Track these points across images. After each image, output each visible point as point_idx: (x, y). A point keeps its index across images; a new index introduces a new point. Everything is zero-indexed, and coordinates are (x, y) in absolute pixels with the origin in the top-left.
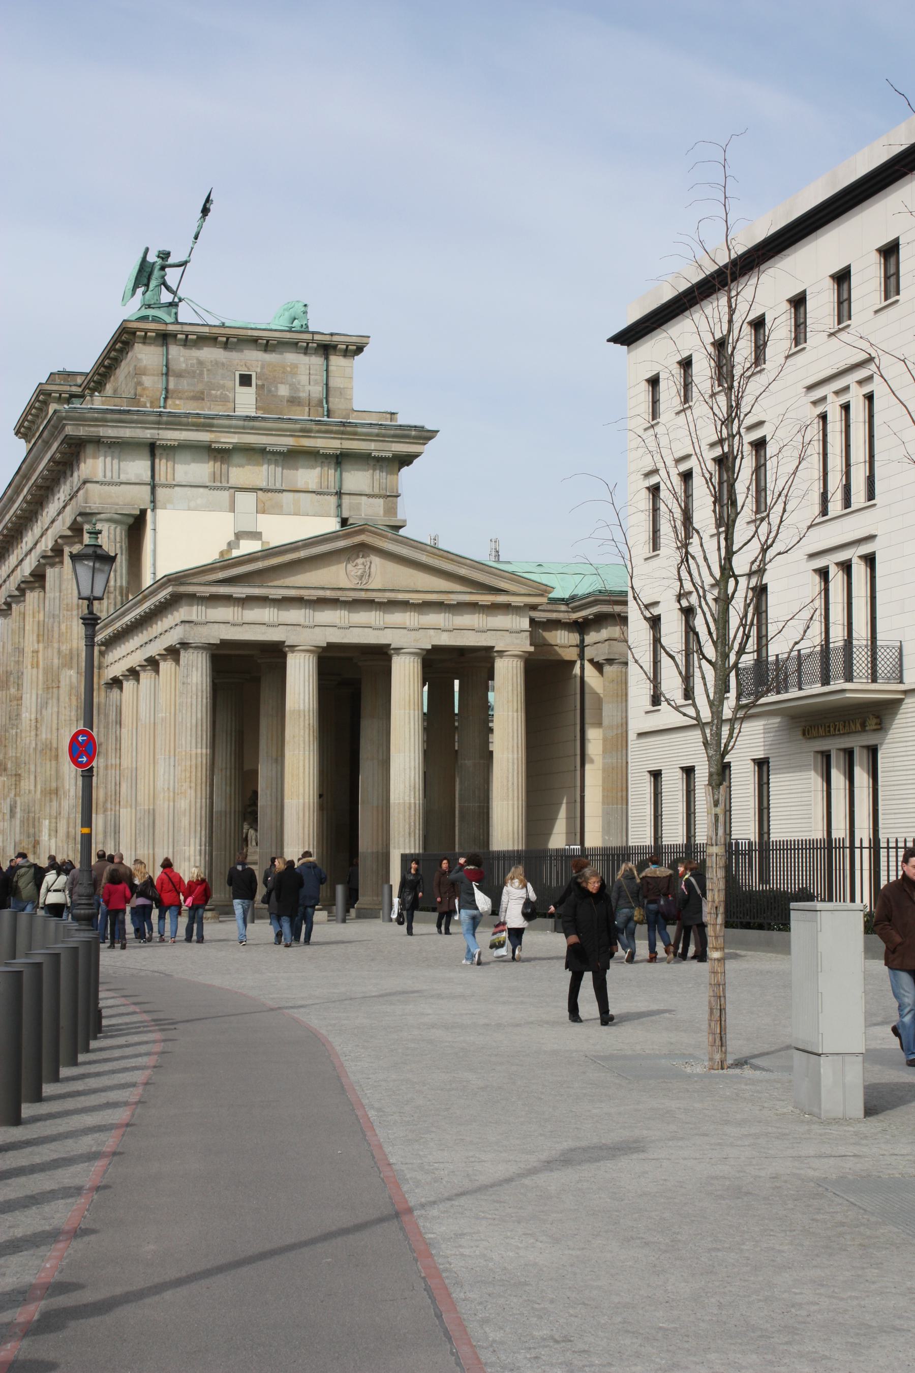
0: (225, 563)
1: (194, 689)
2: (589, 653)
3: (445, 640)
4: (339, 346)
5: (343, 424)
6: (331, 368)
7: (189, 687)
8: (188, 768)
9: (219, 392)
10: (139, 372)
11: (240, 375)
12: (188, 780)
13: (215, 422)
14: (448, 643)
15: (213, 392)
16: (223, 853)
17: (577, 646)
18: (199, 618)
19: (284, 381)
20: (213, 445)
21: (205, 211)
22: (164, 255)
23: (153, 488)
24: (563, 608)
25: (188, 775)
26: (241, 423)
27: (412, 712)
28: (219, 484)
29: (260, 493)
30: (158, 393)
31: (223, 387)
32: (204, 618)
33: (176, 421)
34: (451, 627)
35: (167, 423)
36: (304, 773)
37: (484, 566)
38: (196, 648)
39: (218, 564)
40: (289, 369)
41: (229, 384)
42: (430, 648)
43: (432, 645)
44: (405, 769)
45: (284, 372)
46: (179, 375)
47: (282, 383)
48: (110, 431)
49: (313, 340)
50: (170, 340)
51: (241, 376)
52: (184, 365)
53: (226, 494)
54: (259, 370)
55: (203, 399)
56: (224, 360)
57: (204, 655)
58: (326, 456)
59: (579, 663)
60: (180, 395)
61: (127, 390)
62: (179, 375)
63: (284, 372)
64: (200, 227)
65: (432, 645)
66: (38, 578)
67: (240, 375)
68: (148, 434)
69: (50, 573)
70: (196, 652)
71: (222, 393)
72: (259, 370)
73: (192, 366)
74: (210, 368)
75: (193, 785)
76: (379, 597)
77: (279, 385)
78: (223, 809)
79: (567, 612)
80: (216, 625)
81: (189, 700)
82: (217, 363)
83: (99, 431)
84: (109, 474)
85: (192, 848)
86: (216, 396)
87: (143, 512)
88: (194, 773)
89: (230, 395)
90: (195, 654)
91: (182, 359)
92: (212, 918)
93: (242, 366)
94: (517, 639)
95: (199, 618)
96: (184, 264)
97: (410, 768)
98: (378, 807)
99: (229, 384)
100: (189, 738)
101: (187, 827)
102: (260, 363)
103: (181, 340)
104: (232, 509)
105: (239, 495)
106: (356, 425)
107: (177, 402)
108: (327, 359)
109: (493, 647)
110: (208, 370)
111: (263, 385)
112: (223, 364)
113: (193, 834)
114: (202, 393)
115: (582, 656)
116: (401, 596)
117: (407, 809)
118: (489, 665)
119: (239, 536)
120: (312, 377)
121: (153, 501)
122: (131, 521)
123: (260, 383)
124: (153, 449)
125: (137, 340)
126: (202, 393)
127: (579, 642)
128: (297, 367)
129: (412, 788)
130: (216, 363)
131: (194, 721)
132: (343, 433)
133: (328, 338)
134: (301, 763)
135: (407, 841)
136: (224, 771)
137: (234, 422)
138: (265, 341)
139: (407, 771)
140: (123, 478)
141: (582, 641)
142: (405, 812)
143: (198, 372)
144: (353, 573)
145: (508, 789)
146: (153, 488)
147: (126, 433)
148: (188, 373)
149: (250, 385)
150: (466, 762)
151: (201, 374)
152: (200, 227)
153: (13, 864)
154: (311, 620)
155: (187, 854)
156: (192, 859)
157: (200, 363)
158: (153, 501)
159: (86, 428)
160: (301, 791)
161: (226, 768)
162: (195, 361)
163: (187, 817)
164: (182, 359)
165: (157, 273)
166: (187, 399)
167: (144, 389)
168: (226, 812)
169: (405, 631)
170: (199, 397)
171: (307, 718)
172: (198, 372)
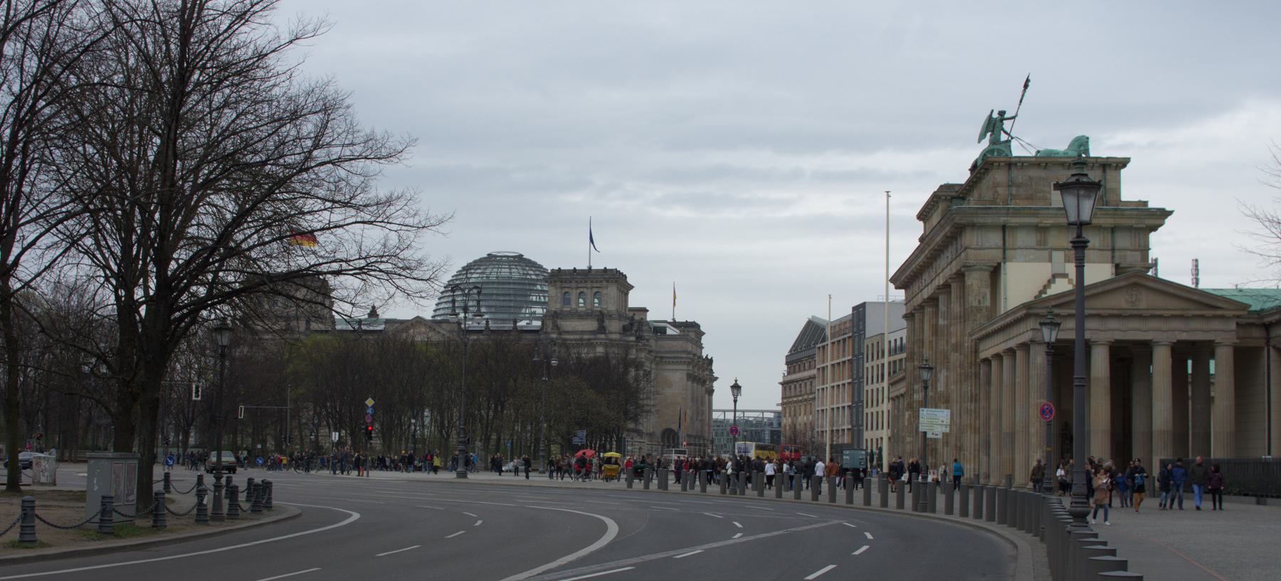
2: (1272, 342)
3: (1184, 336)
5: (1116, 210)
10: (996, 185)
13: (1040, 212)
15: (1038, 195)
20: (1039, 225)
21: (1026, 86)
22: (1002, 113)
23: (1004, 250)
26: (1055, 212)
28: (1042, 247)
29: (1066, 251)
33: (1017, 212)
35: (1013, 213)
50: (1013, 167)
53: (1046, 253)
58: (1106, 229)
61: (988, 195)
62: (1018, 186)
64: (1023, 95)
66: (933, 300)
68: (1002, 220)
69: (942, 298)
84: (980, 244)
87: (999, 264)
96: (1013, 118)
104: (1050, 260)
105: (1054, 253)
106: (1123, 210)
107: (1018, 201)
108: (1104, 171)
112: (1043, 178)
116: (1158, 313)
119: (1054, 276)
121: (1004, 258)
122: (992, 269)
124: (1004, 228)
132: (1115, 215)
133: (1106, 160)
137: (1051, 211)
140: (987, 245)
146: (1004, 250)
147: (989, 220)
152: (1023, 95)
157: (1031, 178)
158: (1004, 258)
162: (1027, 178)
165: (998, 124)
170: (1030, 198)
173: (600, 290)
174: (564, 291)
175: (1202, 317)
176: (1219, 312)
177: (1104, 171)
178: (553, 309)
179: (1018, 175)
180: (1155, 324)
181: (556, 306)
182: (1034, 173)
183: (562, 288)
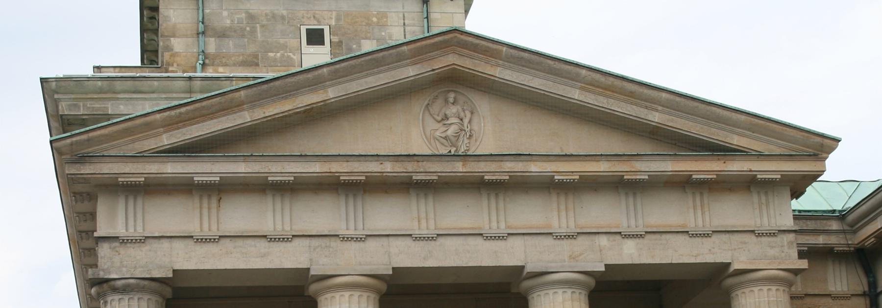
0: (173, 113)
6: (433, 16)
9: (279, 55)
11: (307, 30)
14: (637, 261)
15: (271, 55)
17: (864, 295)
18: (131, 230)
19: (369, 35)
24: (835, 226)
30: (194, 60)
31: (284, 47)
32: (140, 229)
34: (641, 229)
37: (696, 104)
38: (126, 290)
39: (158, 116)
40: (375, 20)
41: (294, 43)
42: (603, 269)
45: (368, 24)
46: (222, 35)
47: (366, 38)
48: (122, 107)
51: (309, 32)
52: (228, 22)
54: (333, 23)
55: (257, 65)
56: (285, 13)
60: (224, 60)
62: (222, 35)
63: (368, 24)
65: (606, 265)
67: (307, 30)
70: (126, 298)
71: (283, 55)
72: (333, 23)
73: (240, 21)
74: (265, 22)
76: (490, 170)
77: (362, 41)
79: (843, 232)
80: (165, 244)
82: (274, 16)
83: (107, 108)
86: (275, 60)
89: (295, 57)
93: (309, 18)
94: (773, 247)
95: (131, 230)
99: (294, 43)
102: (334, 14)
109: (728, 265)
110: (262, 26)
111: (341, 42)
112: (283, 18)
114: (256, 56)
116: (535, 168)
120: (407, 28)
123: (335, 39)
126: (256, 56)
127: (866, 289)
141: (873, 285)
143: (248, 29)
144: (438, 134)
148: (235, 31)
149: (321, 42)
151: (253, 31)
154: (360, 226)
157: (251, 17)
159: (89, 103)
162: (243, 15)
164: (225, 13)
166: (234, 65)
167: (174, 55)
169: (548, 241)
170: (252, 62)
176: (736, 166)
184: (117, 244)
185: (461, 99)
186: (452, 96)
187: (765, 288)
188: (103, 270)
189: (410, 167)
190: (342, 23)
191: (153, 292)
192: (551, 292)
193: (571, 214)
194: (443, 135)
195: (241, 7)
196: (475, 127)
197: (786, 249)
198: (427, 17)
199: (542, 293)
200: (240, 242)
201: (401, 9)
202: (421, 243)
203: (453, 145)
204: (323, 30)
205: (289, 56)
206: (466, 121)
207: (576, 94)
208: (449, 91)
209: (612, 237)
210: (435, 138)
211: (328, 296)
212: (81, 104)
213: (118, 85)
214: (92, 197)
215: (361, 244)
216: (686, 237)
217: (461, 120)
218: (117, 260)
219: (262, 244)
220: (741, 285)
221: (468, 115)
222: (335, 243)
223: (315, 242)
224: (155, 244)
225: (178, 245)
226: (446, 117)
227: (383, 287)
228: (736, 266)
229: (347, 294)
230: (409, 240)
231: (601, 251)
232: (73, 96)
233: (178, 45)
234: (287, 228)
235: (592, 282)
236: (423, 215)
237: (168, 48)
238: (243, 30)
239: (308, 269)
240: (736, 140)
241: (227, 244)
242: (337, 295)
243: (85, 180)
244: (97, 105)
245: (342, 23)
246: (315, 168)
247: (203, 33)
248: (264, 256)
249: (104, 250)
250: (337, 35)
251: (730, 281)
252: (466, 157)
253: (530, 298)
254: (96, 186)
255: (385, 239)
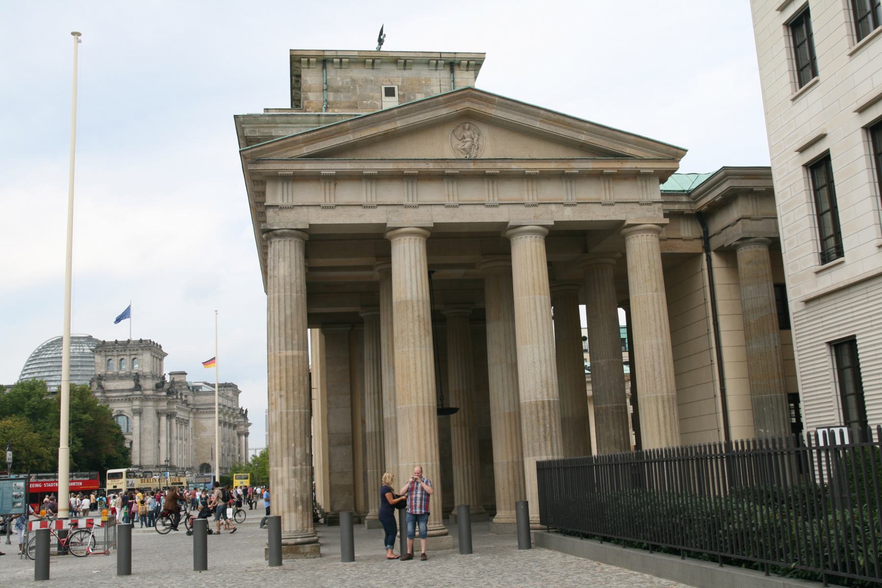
0: (309, 135)
1: (282, 282)
2: (715, 243)
3: (568, 215)
4: (462, 61)
6: (457, 80)
7: (276, 280)
8: (278, 374)
9: (369, 102)
11: (385, 88)
12: (278, 387)
14: (572, 219)
15: (365, 102)
16: (375, 470)
17: (701, 238)
18: (286, 202)
24: (684, 199)
25: (278, 381)
27: (538, 296)
30: (321, 105)
31: (372, 98)
32: (290, 201)
34: (574, 201)
36: (416, 372)
37: (605, 130)
38: (282, 235)
39: (300, 137)
40: (423, 82)
41: (377, 95)
42: (553, 224)
43: (555, 222)
44: (534, 362)
46: (337, 91)
47: (418, 93)
48: (280, 132)
49: (441, 57)
50: (329, 66)
52: (340, 83)
55: (357, 108)
56: (372, 78)
57: (293, 244)
59: (704, 255)
60: (338, 105)
62: (337, 91)
65: (555, 222)
67: (385, 88)
70: (283, 240)
71: (371, 102)
73: (347, 83)
74: (361, 84)
75: (283, 393)
76: (488, 167)
78: (374, 430)
79: (689, 202)
80: (305, 209)
81: (276, 294)
82: (366, 80)
83: (272, 132)
85: (285, 468)
86: (367, 105)
88: (284, 380)
90: (282, 243)
91: (339, 79)
92: (311, 553)
93: (386, 81)
94: (649, 211)
95: (286, 202)
97: (540, 361)
98: (510, 413)
99: (377, 95)
100: (277, 339)
101: (279, 443)
102: (401, 78)
103: (337, 63)
108: (452, 71)
110: (360, 86)
111: (404, 95)
112: (371, 81)
113: (285, 452)
114: (356, 103)
115: (707, 249)
116: (514, 166)
117: (540, 408)
118: (619, 255)
120: (442, 87)
123: (401, 93)
125: (303, 66)
127: (702, 235)
128: (430, 81)
129: (544, 384)
130: (366, 81)
131: (282, 319)
133: (452, 55)
134: (412, 362)
135: (543, 445)
136: (372, 395)
138: (403, 61)
139: (537, 365)
141: (706, 232)
142: (538, 413)
143: (352, 87)
144: (459, 147)
145: (655, 379)
148: (344, 89)
149: (394, 95)
150: (599, 361)
151: (355, 89)
153: (243, 488)
154: (415, 199)
155: (280, 476)
156: (286, 481)
157: (354, 81)
159: (261, 130)
160: (414, 394)
161: (374, 393)
162: (349, 80)
163: (278, 433)
164: (339, 79)
166: (344, 108)
167: (310, 102)
168: (376, 432)
169: (522, 208)
170: (354, 106)
171: (416, 308)
172: (352, 87)
173: (137, 357)
174: (108, 359)
175: (599, 176)
176: (629, 165)
177: (452, 71)
178: (99, 373)
179: (336, 76)
180: (510, 191)
181: (101, 371)
182: (358, 73)
183: (106, 356)
184: (277, 210)
185: (473, 127)
186: (467, 126)
187: (645, 235)
188: (270, 224)
189: (444, 165)
190: (405, 84)
191: (298, 237)
192: (523, 237)
193: (535, 193)
194: (462, 148)
195: (347, 75)
196: (481, 143)
197: (657, 213)
198: (453, 81)
199: (519, 237)
200: (347, 208)
201: (438, 76)
202: (450, 209)
203: (468, 153)
204: (394, 88)
205: (375, 103)
206: (475, 140)
207: (537, 125)
208: (466, 123)
209: (558, 206)
210: (458, 149)
211: (397, 239)
212: (257, 130)
213: (278, 119)
214: (263, 183)
215: (416, 210)
216: (600, 206)
217: (473, 139)
218: (277, 218)
219: (360, 209)
220: (631, 233)
221: (477, 136)
222: (401, 209)
223: (390, 208)
224: (299, 210)
225: (312, 210)
226: (464, 138)
227: (428, 234)
228: (628, 222)
229: (408, 238)
230: (443, 207)
231: (552, 213)
232: (252, 126)
233: (312, 96)
234: (374, 200)
235: (547, 231)
236: (451, 193)
237: (306, 98)
238: (349, 88)
239: (386, 224)
240: (628, 151)
241: (339, 209)
242: (402, 238)
243: (259, 173)
244: (266, 131)
245: (405, 84)
246: (390, 166)
247: (326, 90)
248: (360, 216)
249: (270, 213)
250: (402, 91)
251: (625, 231)
252: (475, 160)
253: (511, 240)
254: (266, 176)
255: (429, 207)
